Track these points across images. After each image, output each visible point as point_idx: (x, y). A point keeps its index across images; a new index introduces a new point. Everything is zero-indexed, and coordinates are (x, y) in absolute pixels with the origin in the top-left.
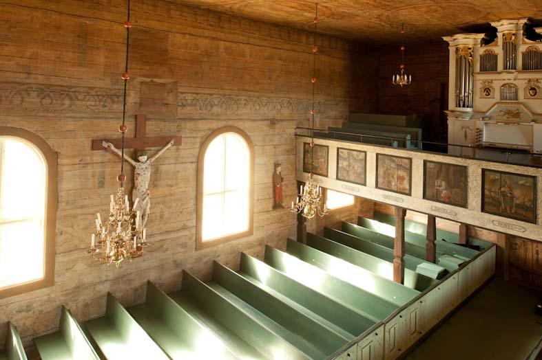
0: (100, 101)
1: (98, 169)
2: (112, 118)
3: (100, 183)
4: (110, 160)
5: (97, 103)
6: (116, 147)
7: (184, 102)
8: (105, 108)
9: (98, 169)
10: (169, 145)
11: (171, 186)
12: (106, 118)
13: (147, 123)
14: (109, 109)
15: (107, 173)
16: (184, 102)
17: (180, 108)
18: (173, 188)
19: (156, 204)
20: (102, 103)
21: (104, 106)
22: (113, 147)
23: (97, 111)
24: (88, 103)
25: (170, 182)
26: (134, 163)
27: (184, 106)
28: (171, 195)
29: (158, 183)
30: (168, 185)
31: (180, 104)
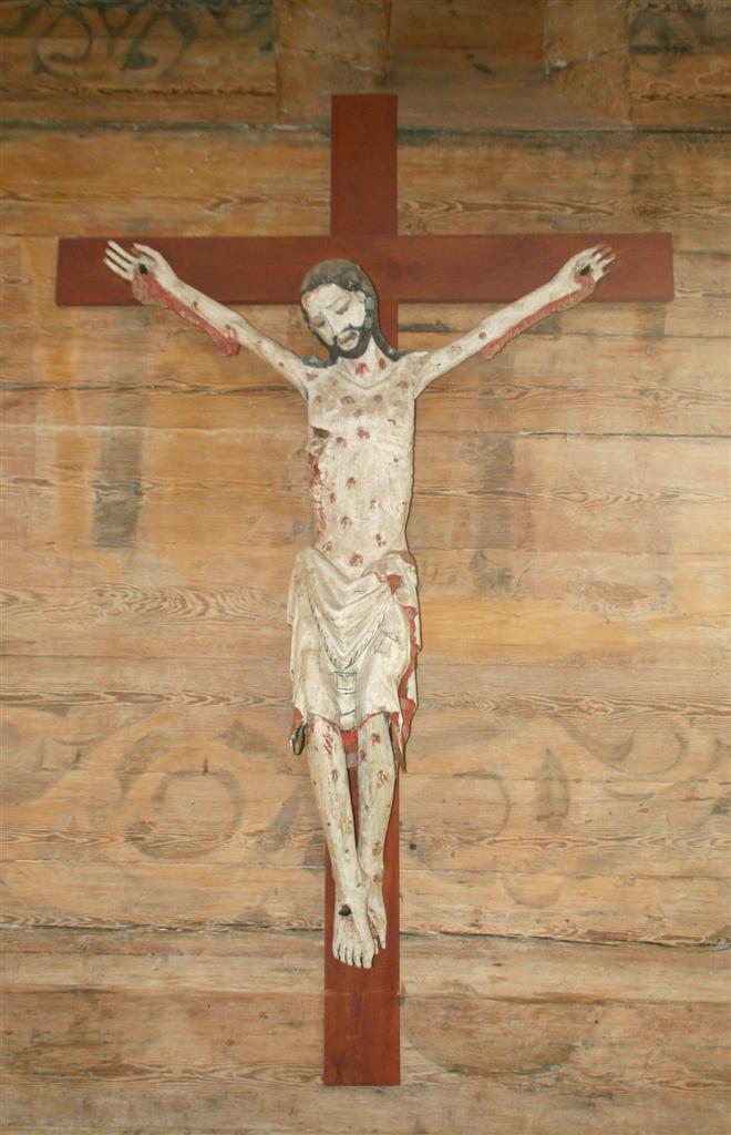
0: (115, 32)
1: (97, 431)
2: (177, 127)
3: (106, 514)
4: (169, 373)
5: (99, 46)
6: (185, 274)
7: (676, 22)
8: (143, 73)
9: (97, 431)
10: (562, 285)
11: (626, 595)
12: (147, 129)
13: (405, 153)
14: (166, 73)
15: (149, 459)
16: (676, 22)
17: (650, 62)
18: (640, 613)
19: (499, 709)
20: (123, 46)
21: (136, 61)
22: (165, 276)
23: (93, 87)
24: (46, 48)
25: (604, 568)
26: (295, 370)
27: (684, 50)
28: (618, 657)
29: (514, 560)
30: (596, 589)
31: (646, 38)
